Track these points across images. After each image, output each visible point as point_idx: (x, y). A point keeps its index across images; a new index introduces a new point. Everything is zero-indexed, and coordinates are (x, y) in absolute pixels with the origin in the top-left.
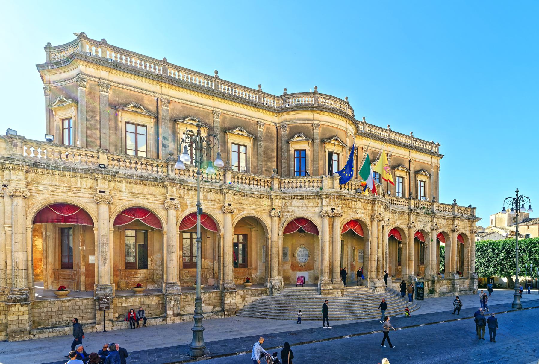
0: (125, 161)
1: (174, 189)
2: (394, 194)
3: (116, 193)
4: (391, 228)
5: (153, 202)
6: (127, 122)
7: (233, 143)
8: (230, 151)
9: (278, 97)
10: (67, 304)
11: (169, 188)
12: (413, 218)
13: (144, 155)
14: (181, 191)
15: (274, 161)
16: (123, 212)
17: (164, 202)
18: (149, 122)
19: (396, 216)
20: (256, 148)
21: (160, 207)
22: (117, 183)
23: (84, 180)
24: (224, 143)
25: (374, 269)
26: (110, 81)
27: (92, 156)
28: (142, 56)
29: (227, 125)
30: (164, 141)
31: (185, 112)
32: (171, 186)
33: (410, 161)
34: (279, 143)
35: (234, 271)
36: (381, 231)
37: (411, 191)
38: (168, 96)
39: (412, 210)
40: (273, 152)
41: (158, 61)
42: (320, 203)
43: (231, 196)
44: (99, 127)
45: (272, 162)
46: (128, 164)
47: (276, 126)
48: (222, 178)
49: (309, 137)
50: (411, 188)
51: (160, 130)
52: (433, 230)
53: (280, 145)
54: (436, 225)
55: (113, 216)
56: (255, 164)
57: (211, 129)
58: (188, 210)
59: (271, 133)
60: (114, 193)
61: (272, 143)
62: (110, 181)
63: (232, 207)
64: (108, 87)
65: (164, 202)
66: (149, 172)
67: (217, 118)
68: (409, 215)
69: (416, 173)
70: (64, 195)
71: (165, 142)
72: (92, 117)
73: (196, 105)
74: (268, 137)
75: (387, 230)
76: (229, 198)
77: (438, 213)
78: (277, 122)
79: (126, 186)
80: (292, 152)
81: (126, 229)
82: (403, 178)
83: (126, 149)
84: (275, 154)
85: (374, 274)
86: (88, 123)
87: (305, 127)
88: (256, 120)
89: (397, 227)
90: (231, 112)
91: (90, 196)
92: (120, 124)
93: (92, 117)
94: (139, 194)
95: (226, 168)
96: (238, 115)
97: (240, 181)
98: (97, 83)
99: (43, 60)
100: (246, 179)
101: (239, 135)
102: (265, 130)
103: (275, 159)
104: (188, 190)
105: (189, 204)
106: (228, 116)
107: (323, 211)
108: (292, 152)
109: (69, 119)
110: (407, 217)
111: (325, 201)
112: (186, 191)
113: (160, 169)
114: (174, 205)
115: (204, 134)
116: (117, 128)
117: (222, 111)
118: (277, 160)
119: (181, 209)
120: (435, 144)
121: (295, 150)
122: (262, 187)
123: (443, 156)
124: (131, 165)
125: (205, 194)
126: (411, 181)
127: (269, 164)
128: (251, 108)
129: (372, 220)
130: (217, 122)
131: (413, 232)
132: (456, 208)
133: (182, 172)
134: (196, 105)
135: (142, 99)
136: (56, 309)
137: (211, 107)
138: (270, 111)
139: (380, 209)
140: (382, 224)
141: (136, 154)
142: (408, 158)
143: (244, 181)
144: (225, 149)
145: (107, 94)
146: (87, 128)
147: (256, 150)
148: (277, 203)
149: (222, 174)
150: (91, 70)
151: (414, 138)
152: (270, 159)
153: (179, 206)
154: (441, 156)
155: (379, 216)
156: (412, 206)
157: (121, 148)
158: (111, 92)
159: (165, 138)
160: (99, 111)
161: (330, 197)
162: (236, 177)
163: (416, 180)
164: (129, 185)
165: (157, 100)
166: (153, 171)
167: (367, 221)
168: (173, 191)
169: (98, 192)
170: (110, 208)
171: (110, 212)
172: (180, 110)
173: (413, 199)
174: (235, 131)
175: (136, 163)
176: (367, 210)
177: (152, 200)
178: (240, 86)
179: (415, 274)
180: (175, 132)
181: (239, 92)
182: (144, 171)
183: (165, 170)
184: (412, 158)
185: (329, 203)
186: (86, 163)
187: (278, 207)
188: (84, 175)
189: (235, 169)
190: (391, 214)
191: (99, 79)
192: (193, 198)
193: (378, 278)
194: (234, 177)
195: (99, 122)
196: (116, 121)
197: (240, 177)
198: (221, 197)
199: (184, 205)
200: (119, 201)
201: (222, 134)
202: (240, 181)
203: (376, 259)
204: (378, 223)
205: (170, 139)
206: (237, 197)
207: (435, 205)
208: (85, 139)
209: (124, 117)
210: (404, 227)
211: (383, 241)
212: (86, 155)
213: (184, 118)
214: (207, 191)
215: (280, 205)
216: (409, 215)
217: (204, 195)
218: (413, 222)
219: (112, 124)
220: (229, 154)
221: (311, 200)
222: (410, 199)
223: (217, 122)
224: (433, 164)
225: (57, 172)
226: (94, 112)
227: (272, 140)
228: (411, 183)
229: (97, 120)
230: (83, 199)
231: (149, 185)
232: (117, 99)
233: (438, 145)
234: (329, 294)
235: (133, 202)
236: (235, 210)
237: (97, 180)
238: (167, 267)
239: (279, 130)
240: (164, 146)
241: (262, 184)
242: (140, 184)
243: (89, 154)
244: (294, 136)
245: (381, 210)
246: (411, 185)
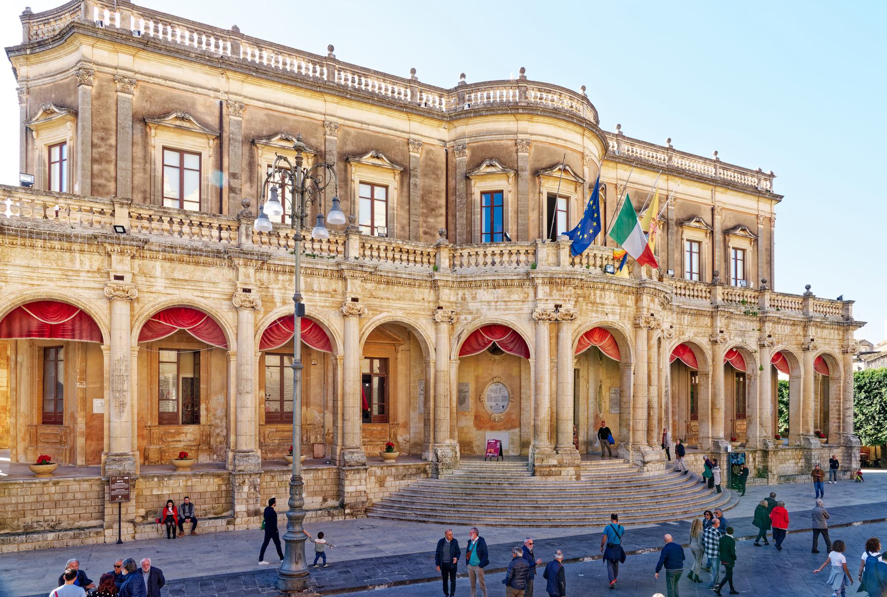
0: (161, 220)
1: (251, 271)
2: (682, 276)
3: (144, 279)
4: (675, 343)
5: (212, 295)
6: (164, 148)
7: (361, 182)
8: (357, 196)
9: (449, 92)
10: (53, 489)
11: (242, 270)
12: (720, 322)
13: (195, 207)
14: (264, 275)
15: (441, 215)
16: (155, 317)
17: (231, 297)
18: (206, 147)
19: (686, 319)
20: (405, 189)
21: (225, 305)
22: (145, 261)
23: (87, 256)
24: (345, 181)
25: (642, 425)
26: (136, 73)
27: (102, 212)
28: (194, 23)
29: (350, 148)
30: (232, 181)
31: (273, 126)
32: (246, 265)
33: (713, 210)
34: (450, 179)
35: (363, 430)
36: (655, 349)
37: (716, 269)
38: (241, 95)
39: (718, 307)
40: (438, 196)
41: (222, 31)
42: (532, 294)
43: (358, 282)
44: (114, 157)
45: (436, 216)
46: (166, 225)
47: (445, 146)
48: (341, 248)
49: (510, 167)
50: (716, 263)
52: (762, 346)
53: (452, 183)
54: (770, 336)
55: (137, 324)
56: (405, 222)
57: (320, 156)
58: (275, 310)
59: (434, 161)
60: (141, 280)
61: (437, 179)
62: (133, 257)
63: (359, 305)
64: (131, 83)
65: (231, 297)
66: (205, 239)
67: (331, 135)
68: (712, 316)
69: (727, 232)
70: (51, 284)
71: (235, 183)
72: (102, 139)
73: (292, 111)
74: (430, 169)
75: (668, 348)
76: (355, 287)
77: (773, 313)
78: (447, 139)
79: (162, 267)
80: (477, 196)
81: (160, 349)
82: (700, 243)
83: (163, 197)
84: (443, 202)
85: (641, 436)
86: (95, 151)
87: (501, 148)
88: (406, 136)
89: (689, 342)
90: (358, 122)
91: (97, 285)
92: (153, 152)
93: (102, 139)
94: (186, 281)
95: (349, 229)
96: (372, 128)
97: (375, 254)
98: (112, 77)
99: (17, 39)
100: (386, 249)
101: (374, 165)
102: (424, 155)
103: (443, 211)
104: (276, 272)
105: (278, 300)
106: (352, 131)
107: (539, 310)
108: (477, 196)
109: (62, 144)
110: (708, 321)
111: (542, 291)
112: (272, 275)
113: (224, 234)
114: (250, 301)
115: (307, 164)
116: (147, 158)
117: (341, 121)
118: (447, 213)
119: (262, 310)
120: (764, 174)
121: (482, 193)
122: (418, 265)
123: (782, 197)
124: (171, 226)
125: (309, 280)
126: (717, 250)
127: (431, 220)
128: (397, 114)
129: (637, 326)
130: (333, 143)
131: (722, 351)
132: (811, 301)
133: (265, 239)
134: (292, 111)
135: (193, 104)
136: (32, 499)
137: (321, 113)
138: (432, 118)
139: (652, 306)
140: (656, 334)
141: (181, 206)
142: (709, 202)
143: (383, 254)
144: (346, 192)
145: (130, 96)
146: (94, 161)
147: (405, 194)
148: (448, 295)
149: (341, 242)
150: (101, 53)
151: (721, 163)
152: (433, 210)
153: (259, 302)
154: (778, 198)
155: (651, 319)
156: (719, 299)
157: (152, 194)
158: (136, 92)
159: (233, 176)
160: (114, 128)
161: (551, 281)
162: (368, 245)
163: (726, 247)
164: (168, 264)
165: (221, 104)
166: (210, 238)
167: (627, 328)
168: (248, 274)
169: (112, 278)
170: (132, 309)
171: (132, 316)
172: (263, 122)
173: (722, 284)
174: (367, 159)
175: (181, 223)
176: (626, 306)
177: (210, 292)
178: (376, 73)
179: (726, 438)
180: (252, 165)
181: (373, 85)
182: (195, 237)
183: (233, 234)
184: (717, 204)
185: (551, 295)
186: (91, 224)
187: (448, 304)
188: (86, 247)
189: (366, 231)
190: (675, 316)
191: (116, 68)
192: (285, 289)
193: (650, 444)
194: (363, 247)
195: (114, 149)
196: (146, 145)
197: (375, 246)
198: (338, 285)
199: (269, 301)
200: (150, 294)
201: (341, 165)
202: (375, 254)
203: (646, 405)
204: (648, 333)
205: (244, 176)
206: (369, 286)
207: (767, 296)
208: (89, 181)
209: (160, 138)
210: (703, 341)
211: (659, 370)
212: (91, 211)
213: (269, 137)
214: (312, 274)
215: (453, 299)
216: (712, 316)
217: (306, 282)
218: (722, 332)
219: (139, 152)
220: (353, 203)
221: (514, 289)
222: (714, 284)
223: (333, 143)
224: (761, 213)
225: (40, 243)
226: (106, 130)
227: (437, 175)
228: (717, 254)
229: (111, 146)
230: (83, 292)
231: (205, 264)
232: (147, 105)
233: (772, 175)
234: (550, 474)
235: (174, 297)
236: (366, 311)
237: (110, 256)
238: (236, 422)
239: (450, 155)
240: (232, 190)
241: (418, 259)
242: (188, 263)
243: (97, 207)
244: (479, 165)
245: (656, 307)
246: (716, 258)
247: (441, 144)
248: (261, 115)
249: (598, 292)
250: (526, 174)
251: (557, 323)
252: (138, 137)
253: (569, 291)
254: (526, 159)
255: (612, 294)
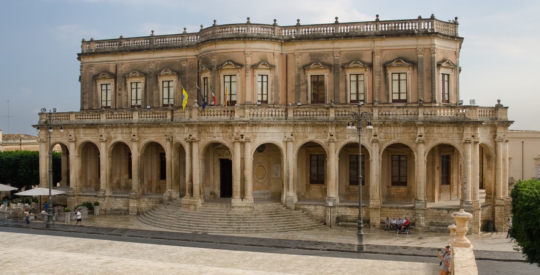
20: (180, 81)
29: (158, 69)
51: (118, 85)
106: (159, 62)
127: (191, 92)
152: (192, 87)
159: (120, 90)
168: (102, 131)
196: (96, 86)
205: (123, 89)
240: (119, 95)
247: (195, 57)
248: (128, 65)
249: (211, 128)
250: (215, 68)
251: (191, 143)
252: (94, 83)
253: (195, 128)
254: (214, 61)
255: (218, 128)
